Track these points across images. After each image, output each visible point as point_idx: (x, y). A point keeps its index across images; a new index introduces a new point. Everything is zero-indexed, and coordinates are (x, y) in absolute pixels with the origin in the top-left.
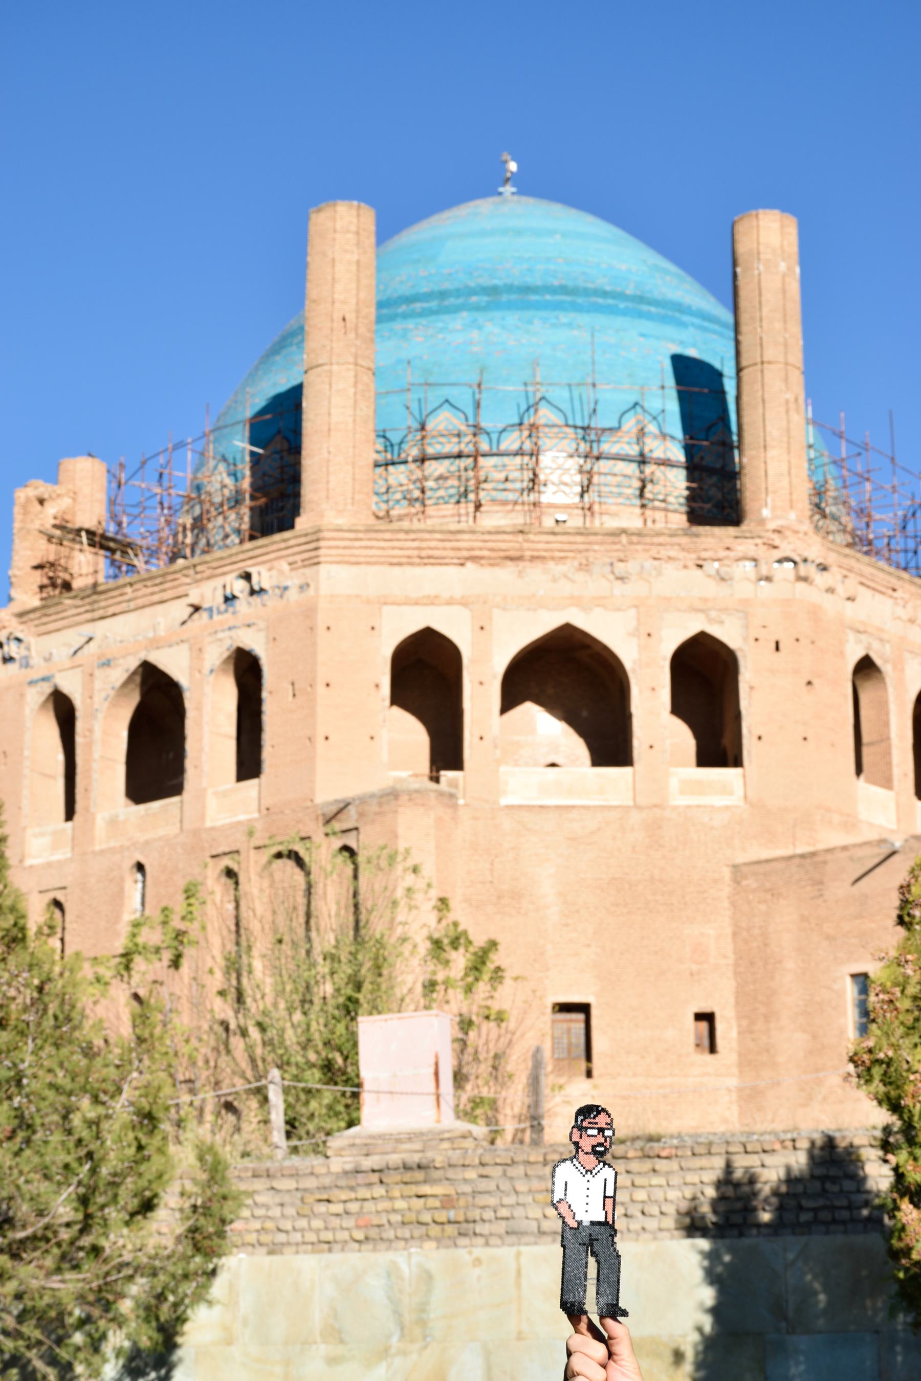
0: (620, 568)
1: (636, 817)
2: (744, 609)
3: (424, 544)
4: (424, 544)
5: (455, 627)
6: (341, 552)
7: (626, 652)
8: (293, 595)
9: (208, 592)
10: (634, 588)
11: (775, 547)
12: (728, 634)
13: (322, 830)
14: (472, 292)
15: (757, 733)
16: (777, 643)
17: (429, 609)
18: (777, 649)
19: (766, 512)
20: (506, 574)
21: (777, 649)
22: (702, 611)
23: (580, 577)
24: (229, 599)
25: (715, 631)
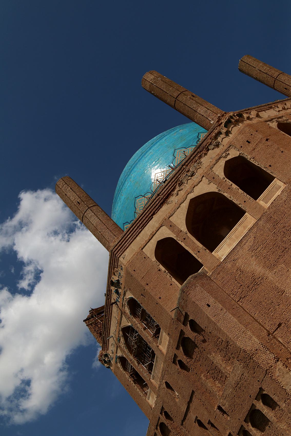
1: (261, 223)
2: (230, 146)
3: (138, 225)
4: (138, 225)
5: (165, 233)
6: (121, 250)
7: (213, 188)
8: (123, 273)
11: (221, 123)
12: (234, 153)
15: (267, 166)
16: (247, 141)
17: (154, 237)
18: (249, 142)
19: (212, 122)
20: (165, 207)
21: (249, 142)
22: (220, 158)
23: (182, 187)
25: (229, 157)
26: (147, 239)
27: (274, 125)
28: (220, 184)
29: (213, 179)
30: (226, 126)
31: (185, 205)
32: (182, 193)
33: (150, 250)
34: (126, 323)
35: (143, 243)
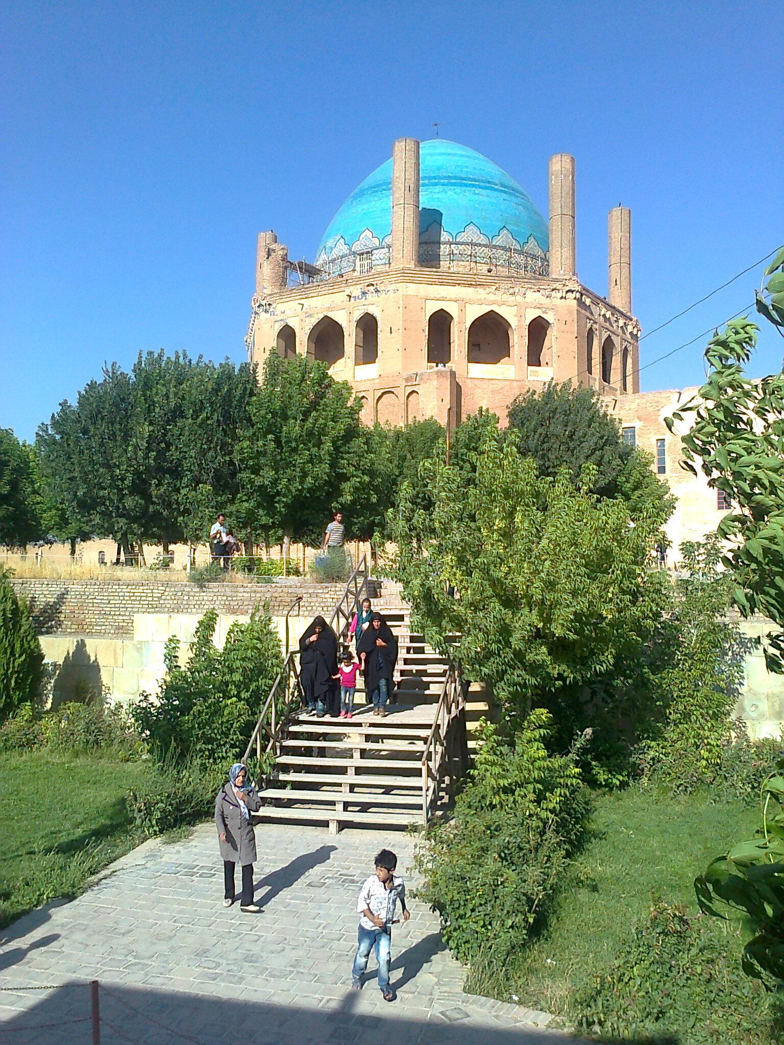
0: (511, 291)
1: (515, 384)
5: (452, 309)
7: (513, 321)
8: (391, 294)
9: (356, 291)
10: (519, 298)
12: (549, 317)
13: (404, 384)
14: (441, 178)
20: (471, 290)
24: (364, 293)
25: (544, 316)
26: (438, 297)
27: (589, 326)
28: (519, 327)
29: (521, 316)
30: (567, 292)
31: (485, 309)
32: (492, 297)
33: (433, 307)
34: (340, 317)
35: (432, 296)
